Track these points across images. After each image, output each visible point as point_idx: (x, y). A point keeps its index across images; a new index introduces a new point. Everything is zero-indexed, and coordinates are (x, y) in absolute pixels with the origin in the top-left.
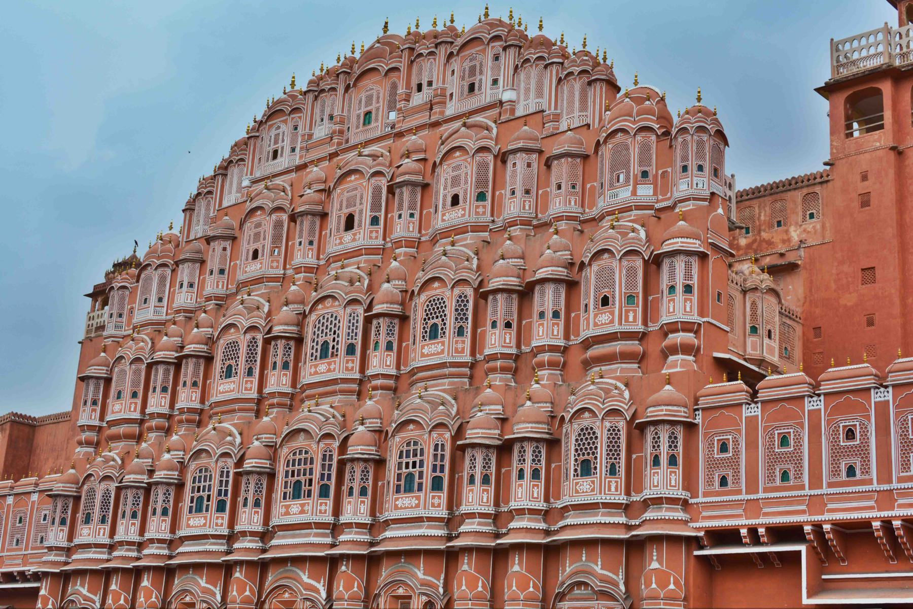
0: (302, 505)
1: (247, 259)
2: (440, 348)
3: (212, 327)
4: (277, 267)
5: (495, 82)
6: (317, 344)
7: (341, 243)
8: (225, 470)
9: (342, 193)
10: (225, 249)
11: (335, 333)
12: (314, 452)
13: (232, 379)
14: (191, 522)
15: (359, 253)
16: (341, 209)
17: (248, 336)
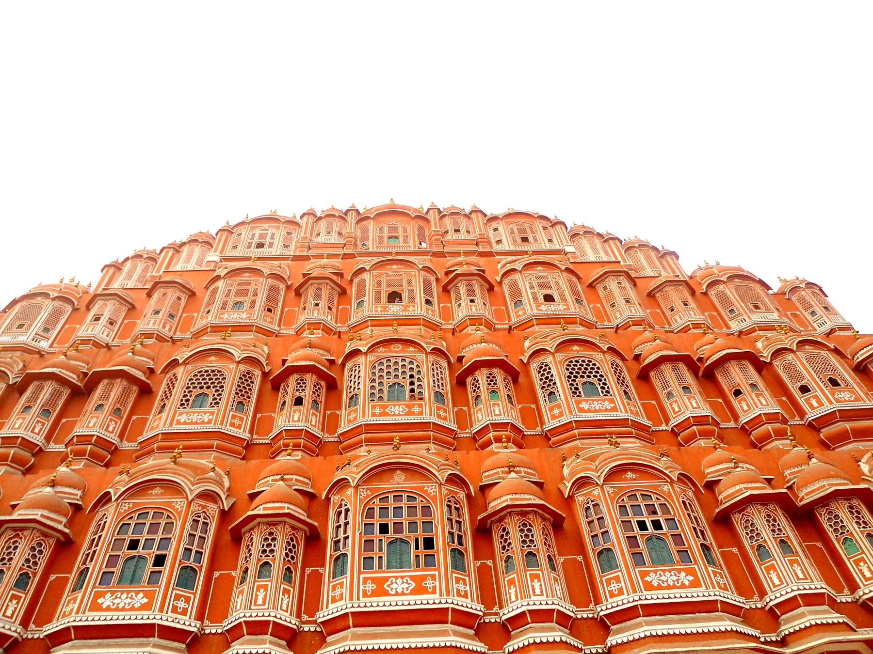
0: (419, 580)
1: (224, 307)
2: (608, 405)
3: (153, 360)
4: (271, 323)
5: (550, 241)
6: (381, 383)
7: (385, 310)
8: (201, 520)
9: (380, 275)
10: (179, 299)
11: (412, 376)
12: (434, 498)
13: (208, 409)
14: (106, 601)
15: (418, 322)
16: (379, 285)
17: (243, 367)
